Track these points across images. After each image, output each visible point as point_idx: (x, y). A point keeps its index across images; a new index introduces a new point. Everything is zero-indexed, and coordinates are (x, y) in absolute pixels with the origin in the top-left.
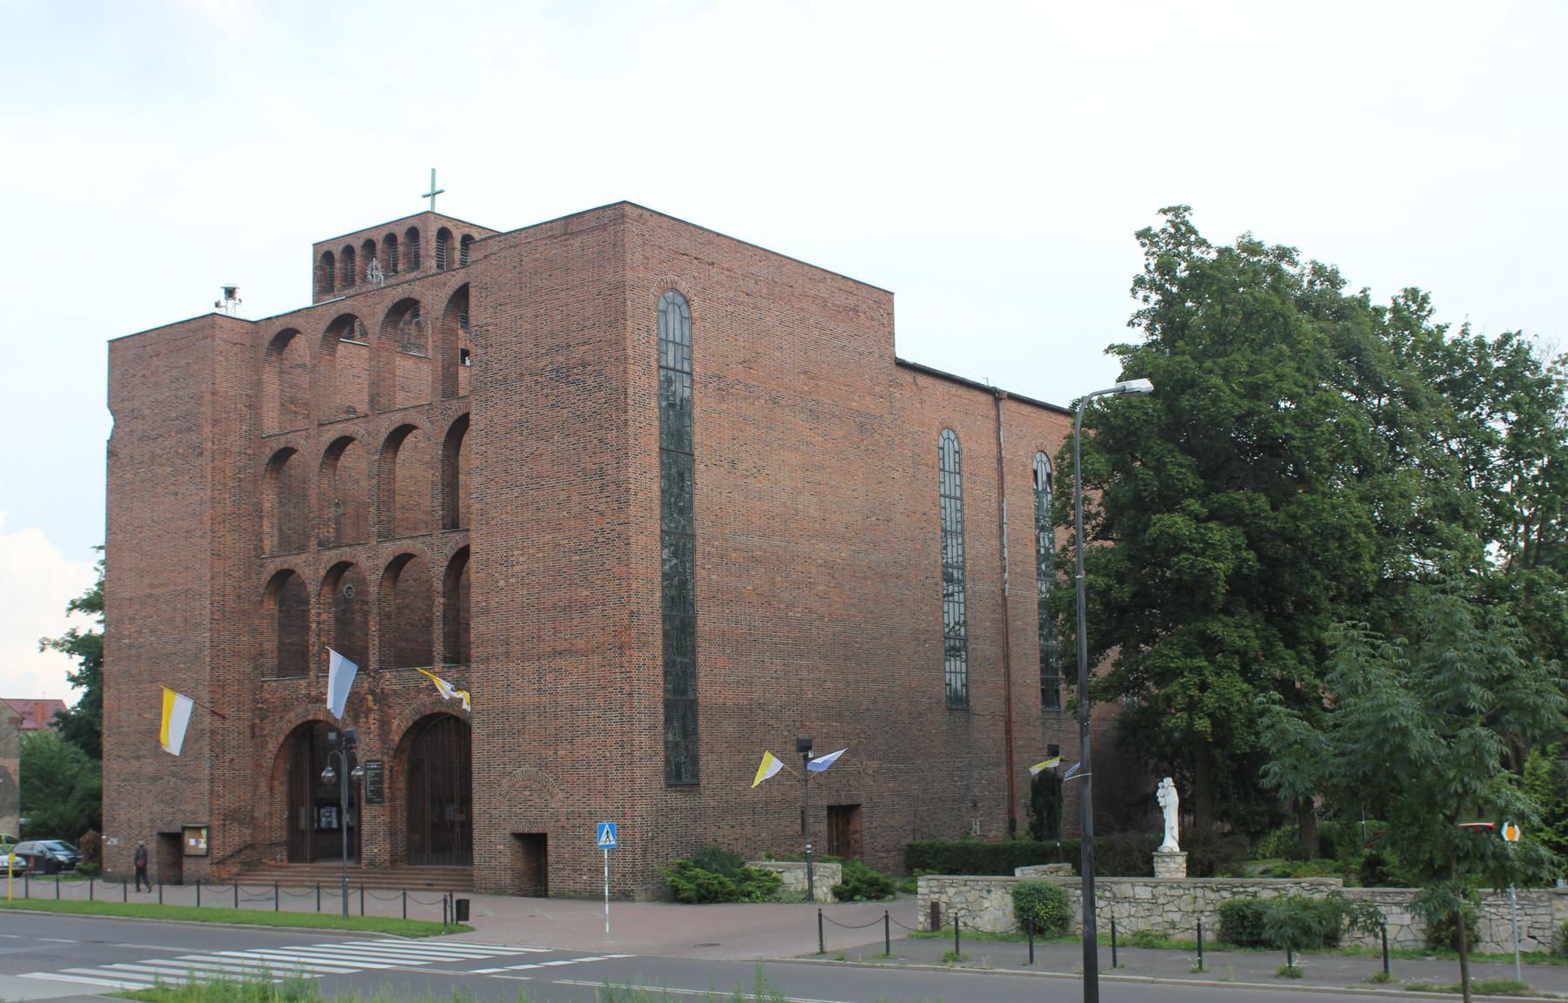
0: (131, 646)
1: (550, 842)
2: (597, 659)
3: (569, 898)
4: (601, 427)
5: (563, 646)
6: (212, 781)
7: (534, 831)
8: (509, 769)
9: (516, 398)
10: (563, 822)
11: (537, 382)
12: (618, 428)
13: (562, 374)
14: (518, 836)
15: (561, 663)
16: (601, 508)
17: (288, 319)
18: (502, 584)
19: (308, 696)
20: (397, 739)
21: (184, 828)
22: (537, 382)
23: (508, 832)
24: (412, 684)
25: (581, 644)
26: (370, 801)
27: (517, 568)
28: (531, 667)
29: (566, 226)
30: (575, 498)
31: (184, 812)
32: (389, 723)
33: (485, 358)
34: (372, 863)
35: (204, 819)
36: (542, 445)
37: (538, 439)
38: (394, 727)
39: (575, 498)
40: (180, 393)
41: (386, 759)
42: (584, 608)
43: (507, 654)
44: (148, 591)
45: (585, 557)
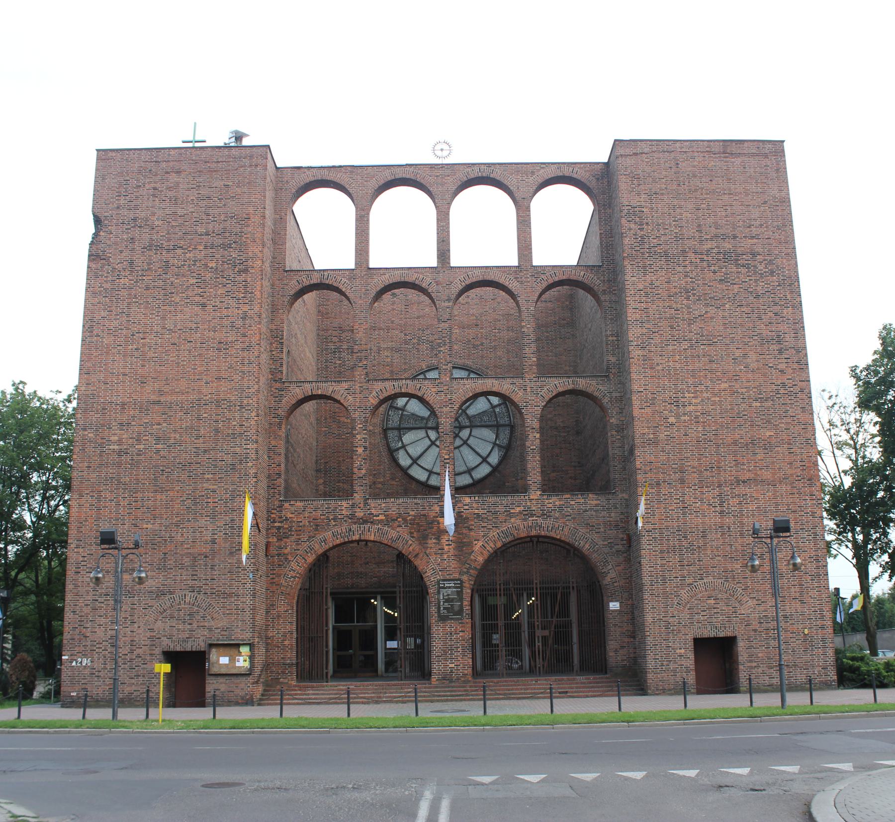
0: (120, 453)
1: (741, 645)
2: (784, 488)
3: (766, 691)
4: (776, 304)
5: (748, 475)
6: (254, 595)
7: (722, 635)
8: (689, 581)
9: (680, 269)
10: (755, 625)
11: (702, 260)
12: (793, 307)
13: (727, 257)
14: (699, 643)
15: (742, 489)
16: (782, 366)
17: (326, 172)
18: (672, 420)
19: (352, 516)
20: (481, 559)
21: (211, 646)
22: (702, 260)
23: (690, 637)
24: (501, 509)
25: (767, 475)
26: (443, 619)
27: (688, 409)
28: (711, 494)
29: (725, 147)
30: (753, 356)
31: (210, 630)
32: (470, 544)
33: (640, 233)
34: (447, 678)
35: (248, 635)
36: (712, 311)
37: (707, 305)
38: (476, 548)
39: (753, 356)
40: (211, 211)
41: (465, 578)
42: (768, 446)
43: (682, 481)
44: (153, 397)
45: (766, 404)
